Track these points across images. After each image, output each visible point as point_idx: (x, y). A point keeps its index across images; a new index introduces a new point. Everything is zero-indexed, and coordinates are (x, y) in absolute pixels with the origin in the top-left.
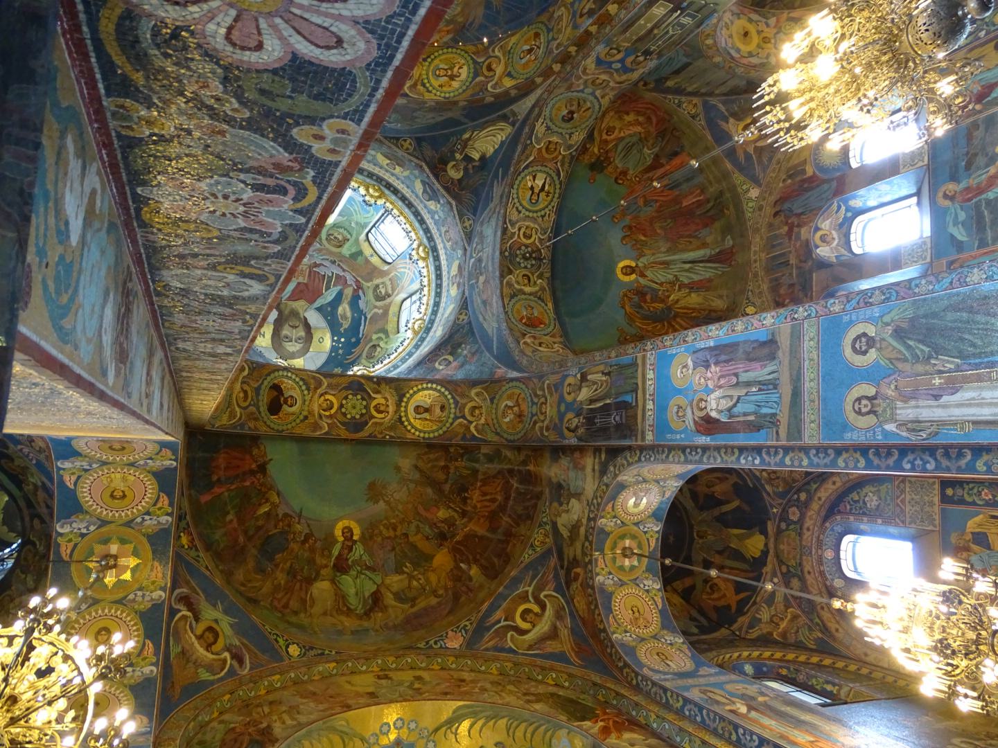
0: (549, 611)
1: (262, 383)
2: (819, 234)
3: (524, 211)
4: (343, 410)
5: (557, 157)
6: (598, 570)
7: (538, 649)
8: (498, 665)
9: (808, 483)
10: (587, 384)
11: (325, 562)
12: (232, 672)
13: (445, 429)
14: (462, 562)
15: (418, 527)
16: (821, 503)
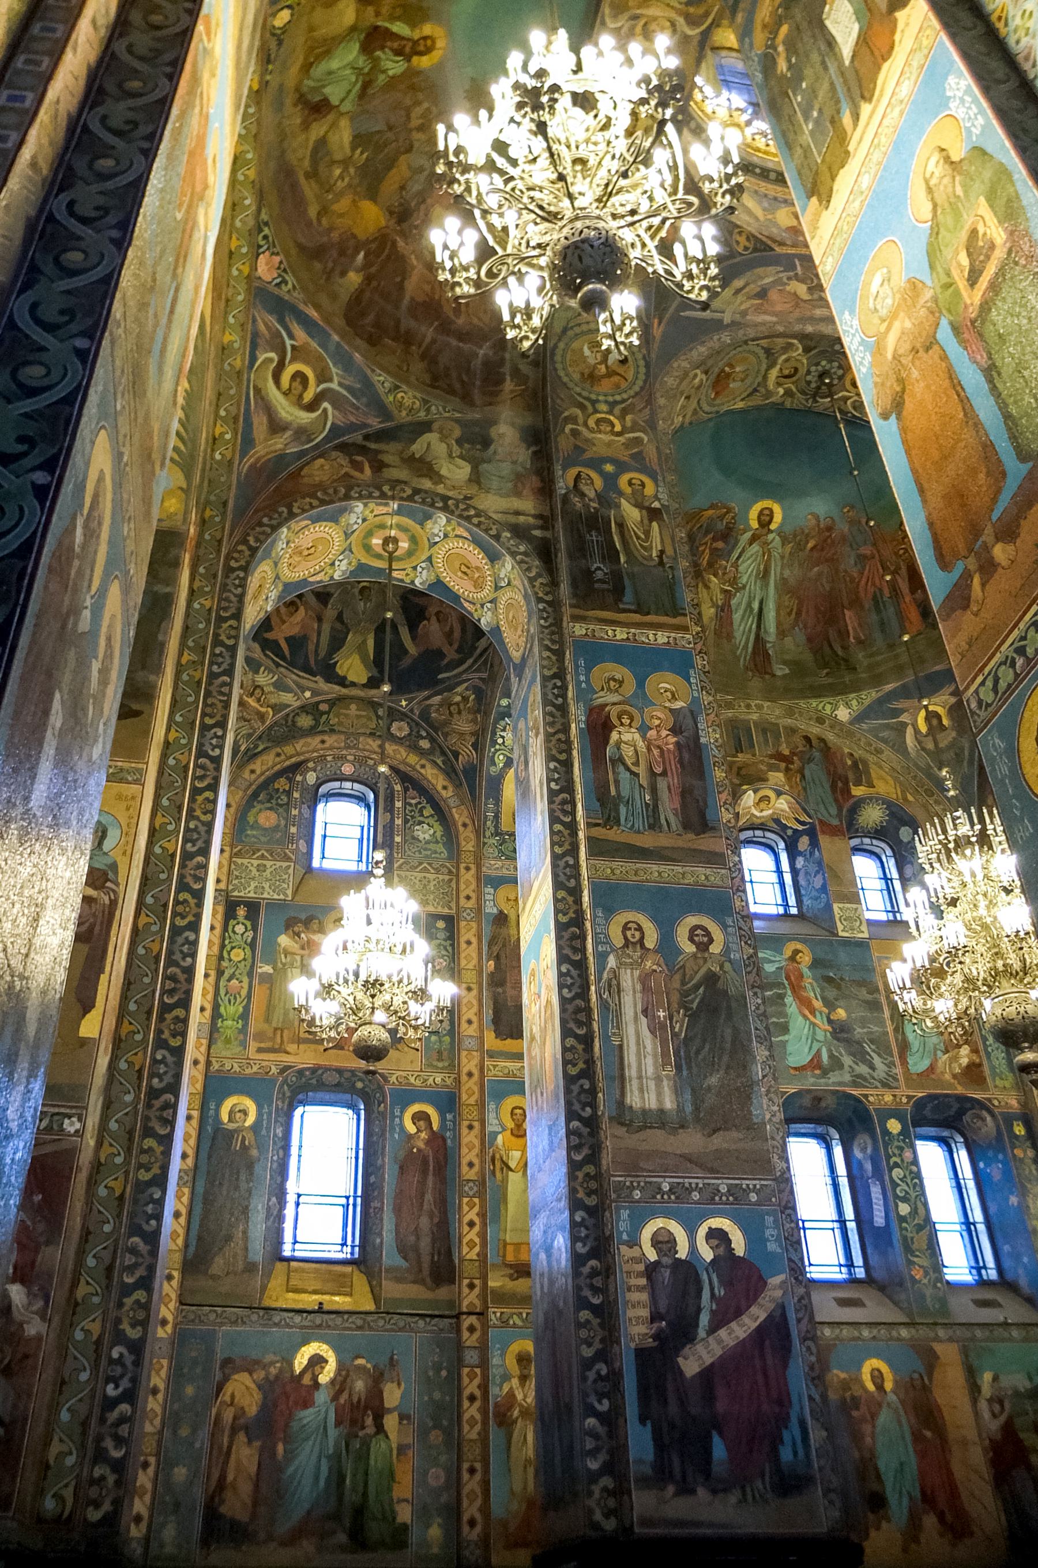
0: (305, 417)
2: (772, 795)
7: (256, 403)
8: (236, 345)
9: (443, 753)
10: (646, 521)
14: (366, 256)
16: (418, 767)
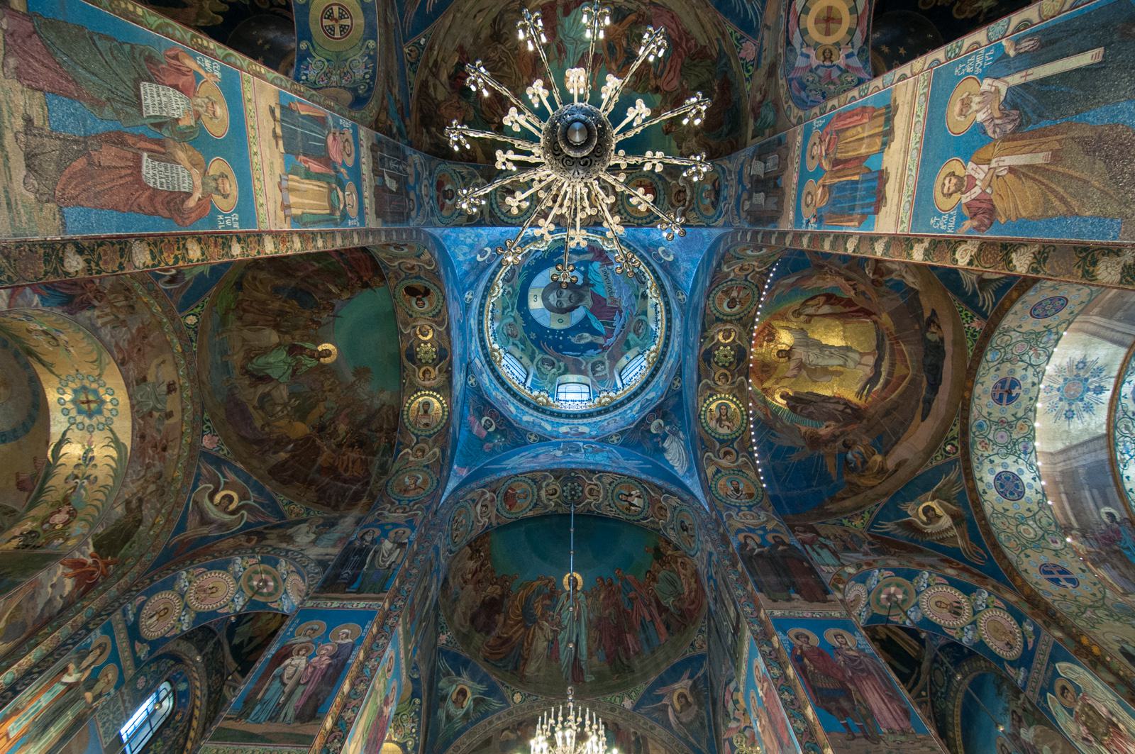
0: (227, 518)
3: (612, 488)
6: (246, 558)
7: (193, 509)
11: (297, 337)
13: (410, 427)
15: (332, 408)
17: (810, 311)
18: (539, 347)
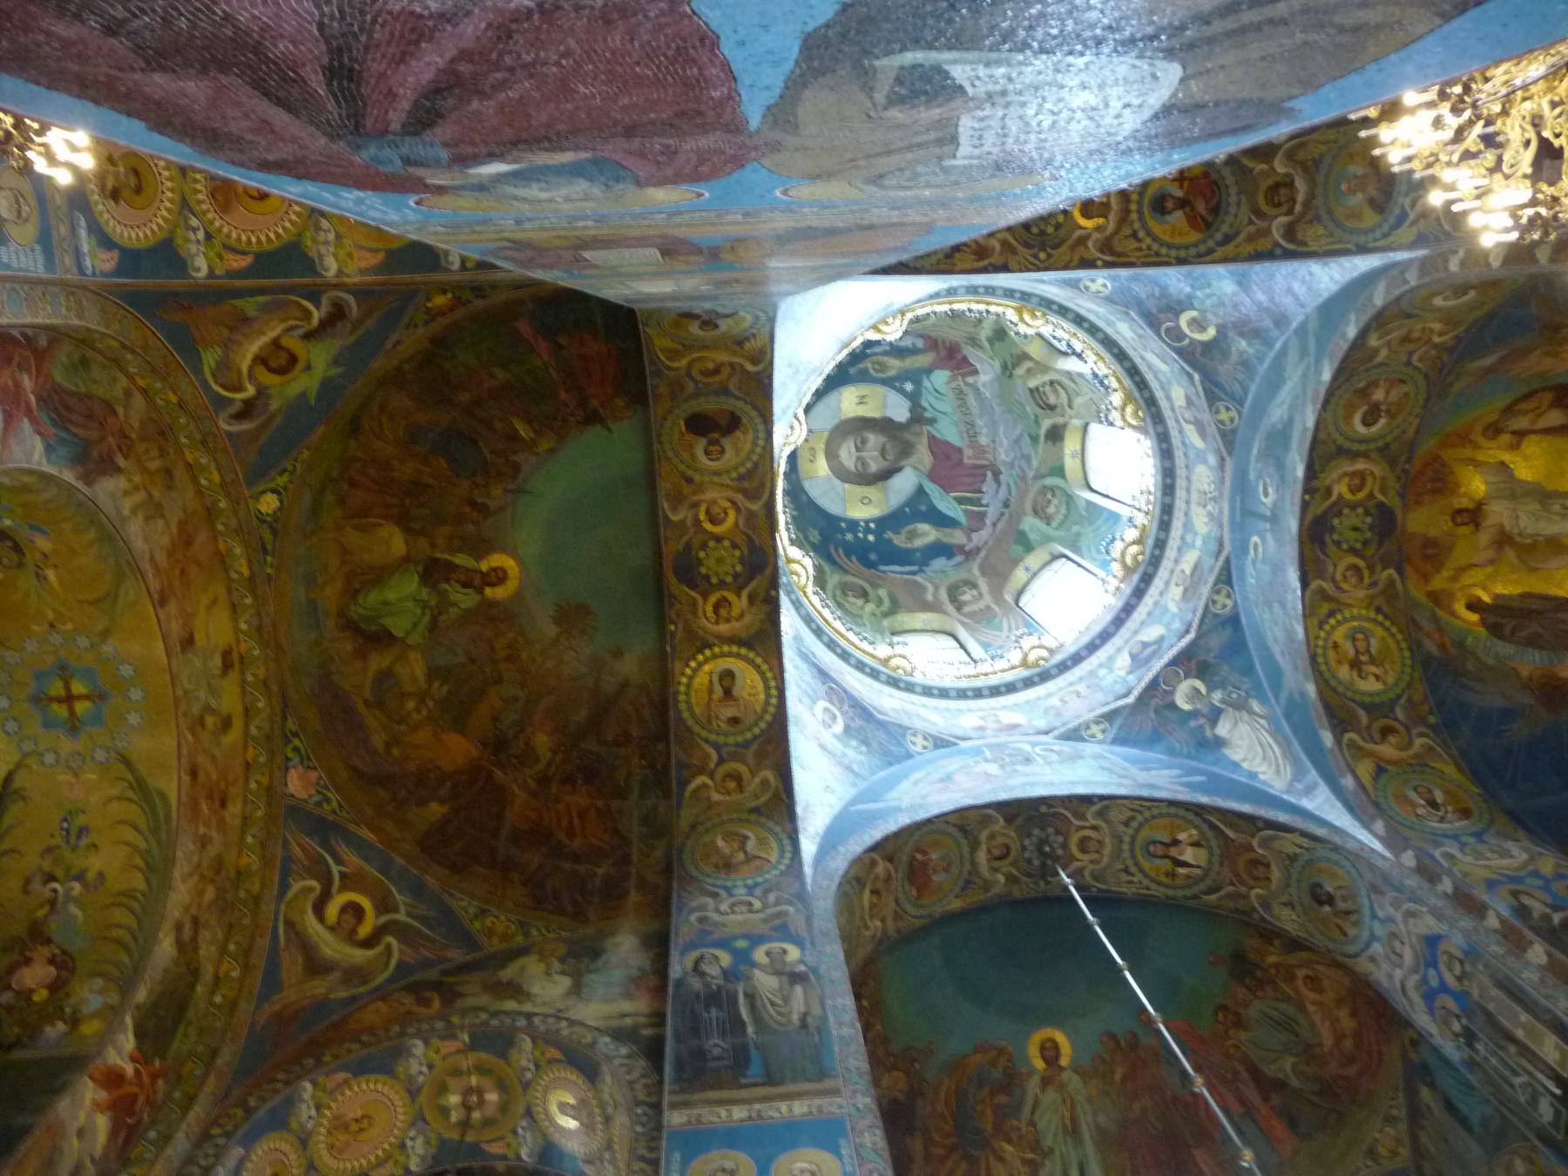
0: (359, 955)
1: (738, 398)
3: (1130, 831)
4: (712, 544)
5: (1242, 882)
7: (288, 940)
8: (254, 868)
11: (440, 542)
12: (221, 402)
13: (697, 729)
15: (516, 699)
17: (1522, 423)
18: (831, 560)
